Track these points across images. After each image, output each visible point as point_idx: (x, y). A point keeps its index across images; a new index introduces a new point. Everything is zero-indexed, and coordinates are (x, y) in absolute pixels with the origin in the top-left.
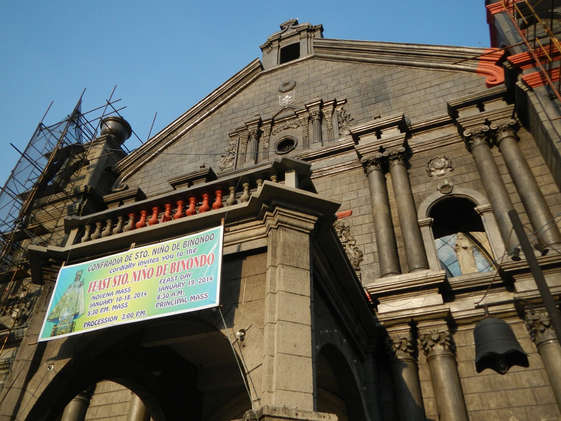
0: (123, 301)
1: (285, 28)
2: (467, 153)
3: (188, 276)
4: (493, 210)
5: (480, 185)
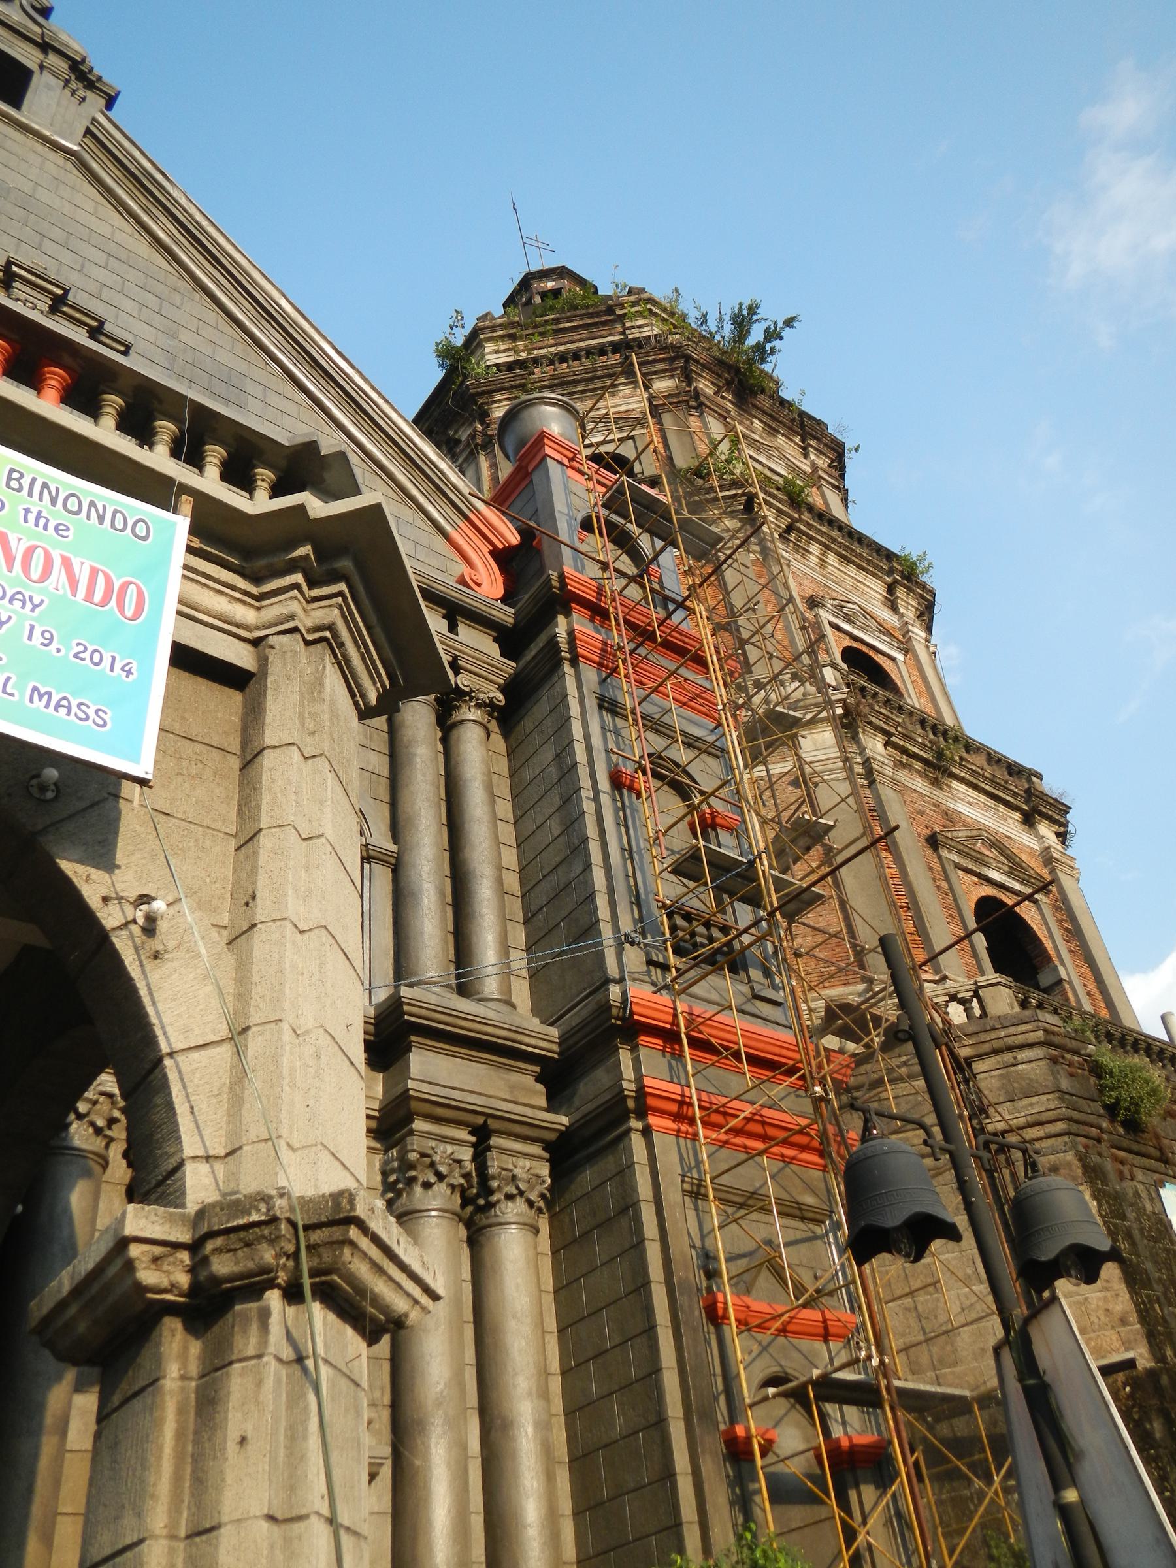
3: (29, 606)
5: (384, 793)
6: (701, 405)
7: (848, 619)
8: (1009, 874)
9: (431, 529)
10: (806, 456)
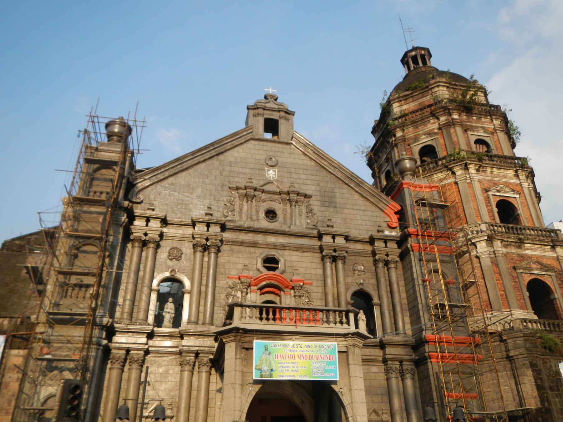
0: (295, 369)
1: (268, 99)
2: (373, 265)
4: (380, 305)
5: (376, 288)
7: (499, 191)
8: (541, 270)
9: (379, 211)
10: (492, 121)
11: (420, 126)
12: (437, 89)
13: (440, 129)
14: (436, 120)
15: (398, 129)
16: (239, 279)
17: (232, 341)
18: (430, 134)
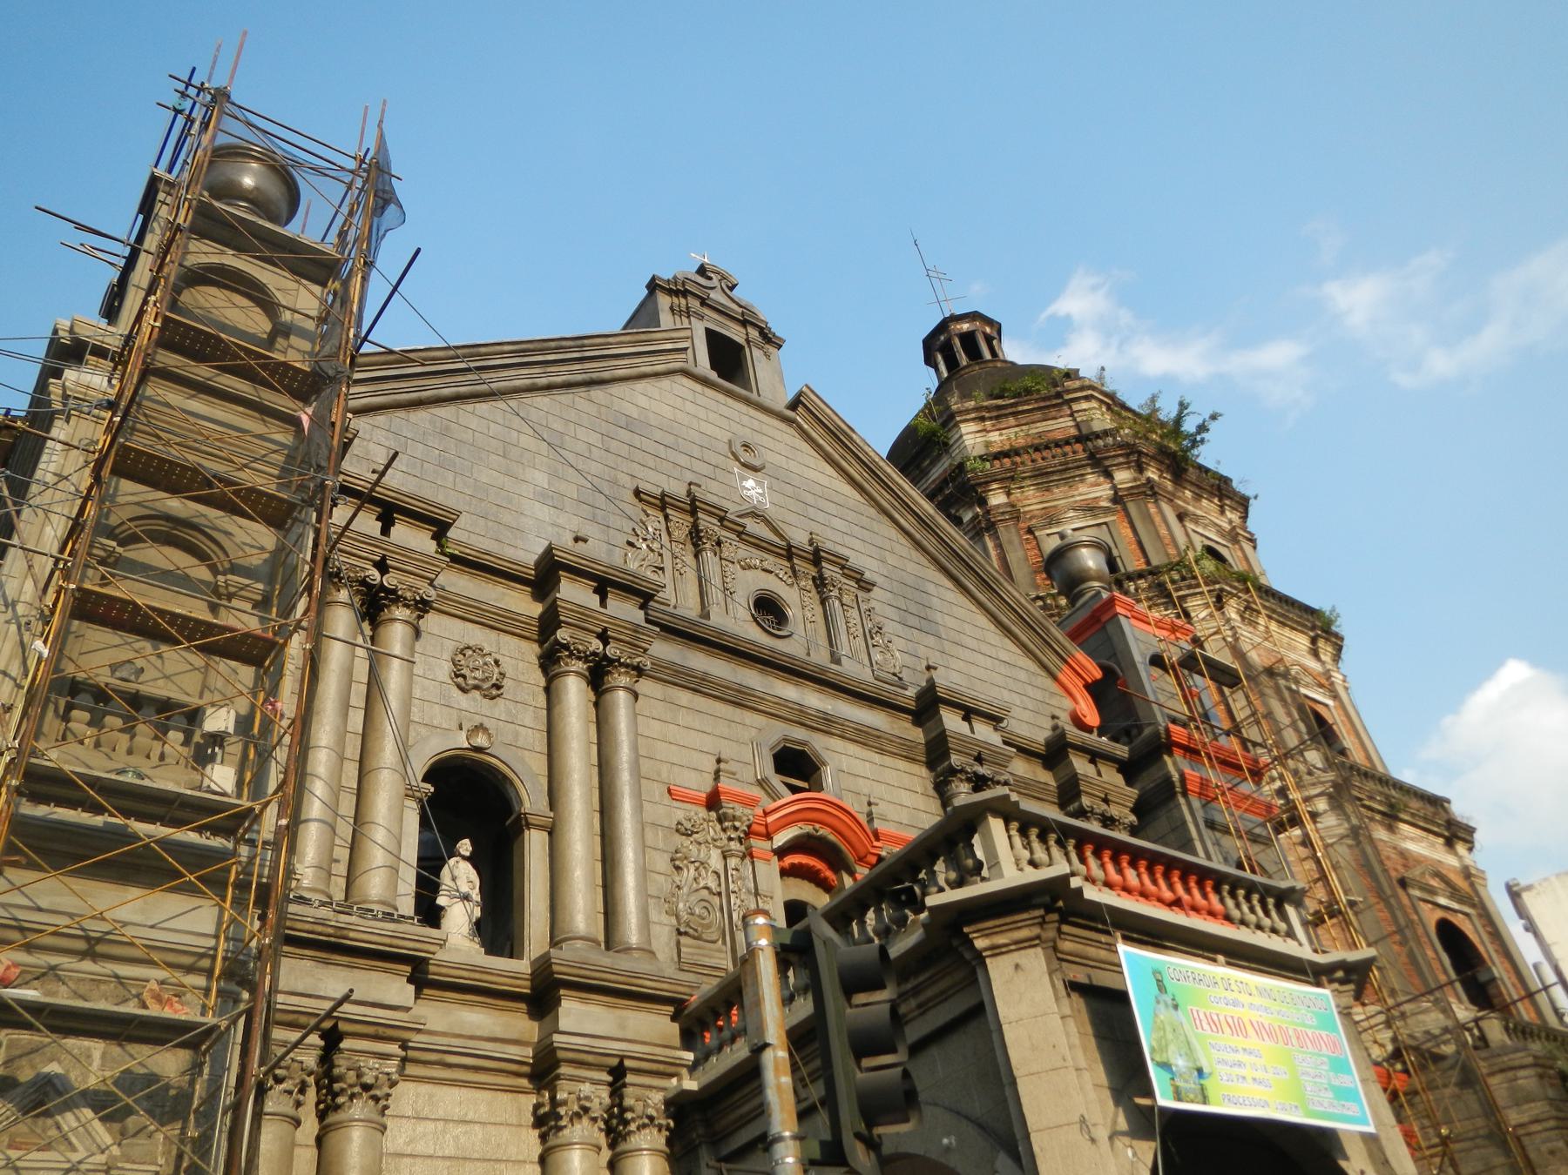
1: (710, 279)
6: (1155, 494)
8: (1452, 897)
10: (1222, 512)
11: (1058, 487)
12: (1084, 405)
13: (1117, 499)
14: (1102, 479)
15: (995, 486)
16: (713, 801)
17: (1022, 945)
18: (1091, 509)
